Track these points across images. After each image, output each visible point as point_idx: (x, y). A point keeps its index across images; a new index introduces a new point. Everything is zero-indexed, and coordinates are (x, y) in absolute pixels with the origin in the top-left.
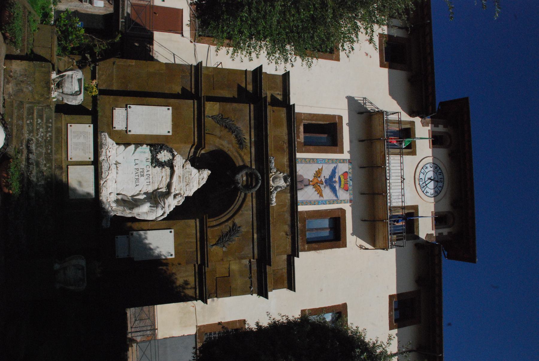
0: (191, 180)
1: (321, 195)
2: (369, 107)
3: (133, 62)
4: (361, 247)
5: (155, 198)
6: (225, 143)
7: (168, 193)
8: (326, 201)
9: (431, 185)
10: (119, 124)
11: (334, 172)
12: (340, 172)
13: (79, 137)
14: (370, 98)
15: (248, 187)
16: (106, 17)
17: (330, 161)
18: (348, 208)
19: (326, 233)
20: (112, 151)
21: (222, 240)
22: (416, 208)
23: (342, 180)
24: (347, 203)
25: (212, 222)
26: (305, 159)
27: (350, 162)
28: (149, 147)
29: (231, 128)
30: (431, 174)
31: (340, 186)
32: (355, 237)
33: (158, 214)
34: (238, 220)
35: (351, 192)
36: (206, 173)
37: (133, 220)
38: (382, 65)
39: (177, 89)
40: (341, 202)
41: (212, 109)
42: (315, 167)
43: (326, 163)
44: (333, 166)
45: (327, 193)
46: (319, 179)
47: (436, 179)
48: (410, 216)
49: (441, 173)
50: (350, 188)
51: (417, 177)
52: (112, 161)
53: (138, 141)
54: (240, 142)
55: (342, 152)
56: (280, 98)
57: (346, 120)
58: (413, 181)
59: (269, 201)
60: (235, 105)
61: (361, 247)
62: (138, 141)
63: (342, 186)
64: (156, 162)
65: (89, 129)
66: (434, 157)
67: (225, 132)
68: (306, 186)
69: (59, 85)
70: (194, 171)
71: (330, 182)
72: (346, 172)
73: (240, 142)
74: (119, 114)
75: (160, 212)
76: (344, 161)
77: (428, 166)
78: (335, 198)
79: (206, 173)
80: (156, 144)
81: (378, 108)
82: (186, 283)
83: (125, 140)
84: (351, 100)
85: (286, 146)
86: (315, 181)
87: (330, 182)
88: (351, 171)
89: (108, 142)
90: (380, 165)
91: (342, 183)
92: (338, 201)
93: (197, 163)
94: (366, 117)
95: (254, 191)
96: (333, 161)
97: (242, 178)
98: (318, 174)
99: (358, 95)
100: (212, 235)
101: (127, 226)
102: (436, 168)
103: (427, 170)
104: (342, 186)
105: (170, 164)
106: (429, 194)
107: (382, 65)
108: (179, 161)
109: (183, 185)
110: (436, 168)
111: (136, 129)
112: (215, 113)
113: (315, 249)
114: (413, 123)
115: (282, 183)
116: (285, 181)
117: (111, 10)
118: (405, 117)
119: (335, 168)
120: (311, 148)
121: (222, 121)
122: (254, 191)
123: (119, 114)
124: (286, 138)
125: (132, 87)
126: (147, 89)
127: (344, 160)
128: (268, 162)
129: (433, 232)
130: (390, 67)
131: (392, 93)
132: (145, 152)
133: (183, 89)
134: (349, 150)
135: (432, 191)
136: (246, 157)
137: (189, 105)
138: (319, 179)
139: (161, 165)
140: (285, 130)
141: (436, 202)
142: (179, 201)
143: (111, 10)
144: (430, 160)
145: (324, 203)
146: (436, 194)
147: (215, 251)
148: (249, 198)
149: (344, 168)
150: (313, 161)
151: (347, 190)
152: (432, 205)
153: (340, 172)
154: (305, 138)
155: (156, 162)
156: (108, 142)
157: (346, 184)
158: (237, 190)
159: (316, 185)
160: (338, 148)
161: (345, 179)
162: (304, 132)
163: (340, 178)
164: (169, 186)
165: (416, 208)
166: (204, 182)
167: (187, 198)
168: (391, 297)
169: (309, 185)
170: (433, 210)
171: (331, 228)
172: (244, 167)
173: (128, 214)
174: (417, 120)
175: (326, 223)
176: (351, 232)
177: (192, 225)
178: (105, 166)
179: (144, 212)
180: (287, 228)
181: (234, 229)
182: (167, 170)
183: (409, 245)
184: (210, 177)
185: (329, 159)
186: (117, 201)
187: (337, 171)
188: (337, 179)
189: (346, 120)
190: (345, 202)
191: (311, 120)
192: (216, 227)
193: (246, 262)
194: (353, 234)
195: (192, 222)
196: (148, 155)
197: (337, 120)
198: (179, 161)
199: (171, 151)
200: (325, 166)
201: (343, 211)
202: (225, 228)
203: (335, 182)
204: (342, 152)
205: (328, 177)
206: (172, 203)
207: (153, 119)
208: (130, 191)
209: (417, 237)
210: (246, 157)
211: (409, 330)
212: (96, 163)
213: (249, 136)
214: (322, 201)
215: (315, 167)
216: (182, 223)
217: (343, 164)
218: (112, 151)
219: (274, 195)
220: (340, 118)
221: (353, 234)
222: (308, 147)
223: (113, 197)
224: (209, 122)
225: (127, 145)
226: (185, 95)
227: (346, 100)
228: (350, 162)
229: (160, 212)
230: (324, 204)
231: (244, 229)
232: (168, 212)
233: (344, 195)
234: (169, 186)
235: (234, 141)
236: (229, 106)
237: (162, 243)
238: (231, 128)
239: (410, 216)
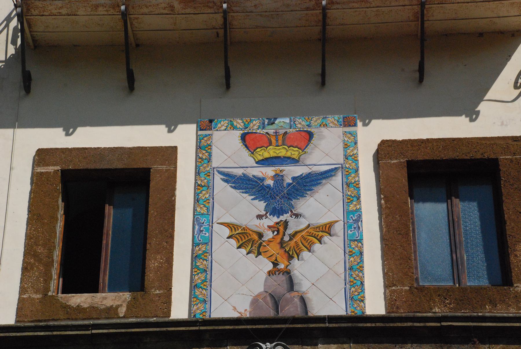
1: (327, 229)
8: (347, 213)
12: (244, 163)
17: (204, 195)
18: (372, 134)
19: (470, 213)
23: (271, 152)
24: (354, 135)
26: (193, 286)
27: (206, 125)
31: (295, 161)
32: (482, 107)
35: (316, 121)
40: (351, 157)
42: (225, 251)
43: (210, 211)
45: (319, 207)
46: (269, 235)
50: (301, 123)
55: (170, 154)
57: (54, 138)
63: (294, 153)
68: (291, 284)
71: (280, 197)
72: (243, 137)
76: (203, 148)
81: (9, 19)
86: (274, 249)
87: (280, 197)
88: (239, 123)
90: (219, 18)
91: (282, 152)
92: (349, 170)
96: (203, 188)
98: (248, 240)
104: (294, 153)
119: (229, 178)
120: (153, 263)
127: (199, 147)
134: (162, 129)
138: (269, 235)
145: (354, 219)
149: (228, 147)
151: (310, 135)
153: (244, 163)
154: (112, 289)
157: (285, 139)
159: (290, 246)
162: (93, 287)
169: (287, 273)
171: (449, 195)
175: (430, 214)
176: (463, 120)
185: (197, 200)
187: (239, 172)
188: (269, 172)
189: (54, 138)
190: (350, 145)
191: (49, 265)
194: (473, 115)
197: (51, 169)
200: (221, 214)
201: (385, 150)
203: (278, 178)
204: (170, 154)
205: (261, 205)
214: (347, 226)
215: (225, 251)
217: (215, 151)
220: (43, 156)
221: (473, 115)
222: (150, 276)
228: (206, 125)
230: (359, 219)
233: (326, 148)
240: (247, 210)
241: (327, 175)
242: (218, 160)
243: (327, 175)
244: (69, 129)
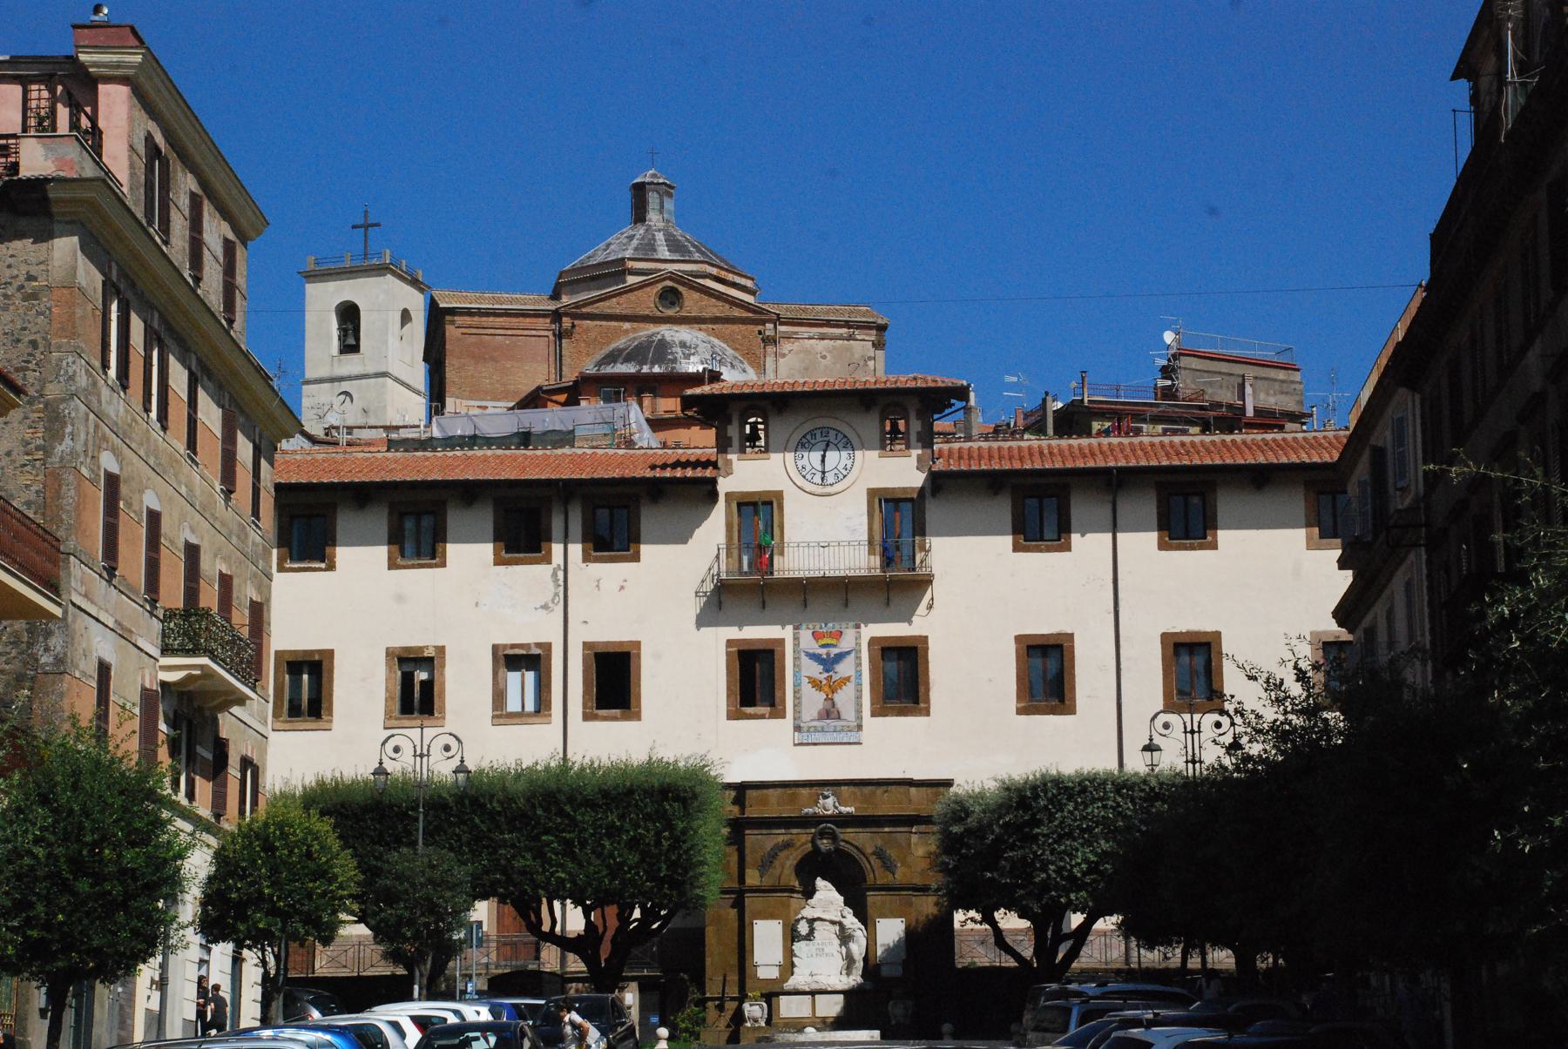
0: (827, 899)
1: (848, 679)
4: (930, 607)
5: (845, 937)
6: (788, 863)
7: (840, 924)
9: (832, 456)
11: (815, 657)
14: (695, 586)
15: (834, 837)
16: (642, 990)
21: (889, 867)
23: (825, 641)
25: (870, 878)
28: (797, 947)
29: (773, 855)
32: (914, 619)
34: (869, 850)
36: (820, 882)
38: (636, 558)
40: (858, 644)
41: (753, 878)
44: (805, 660)
45: (844, 669)
47: (823, 445)
48: (887, 503)
49: (812, 433)
51: (820, 490)
54: (787, 845)
55: (781, 642)
56: (733, 794)
57: (734, 633)
58: (826, 509)
59: (849, 815)
60: (747, 851)
61: (930, 607)
64: (809, 937)
66: (785, 449)
67: (777, 863)
68: (834, 705)
70: (817, 896)
71: (829, 663)
73: (787, 845)
76: (796, 638)
77: (800, 463)
79: (820, 882)
80: (792, 936)
84: (703, 621)
85: (789, 791)
87: (829, 663)
91: (829, 641)
93: (809, 892)
94: (723, 599)
95: (838, 830)
97: (825, 844)
98: (816, 684)
99: (693, 607)
100: (882, 878)
102: (803, 446)
103: (808, 468)
105: (811, 921)
106: (849, 463)
107: (636, 558)
108: (808, 912)
109: (832, 908)
110: (803, 445)
112: (757, 873)
113: (928, 690)
118: (720, 507)
119: (808, 654)
120: (778, 694)
122: (838, 830)
128: (807, 817)
130: (638, 541)
131: (683, 538)
133: (733, 907)
135: (844, 454)
136: (802, 839)
137: (751, 902)
140: (771, 791)
141: (864, 446)
142: (848, 912)
143: (634, 985)
144: (790, 456)
145: (859, 675)
146: (848, 445)
147: (901, 875)
148: (846, 837)
149: (806, 635)
150: (796, 692)
155: (809, 937)
157: (831, 635)
158: (838, 851)
160: (778, 649)
161: (823, 636)
163: (823, 646)
164: (833, 923)
166: (830, 886)
167: (846, 903)
168: (1017, 548)
172: (813, 841)
181: (880, 854)
182: (817, 924)
183: (934, 512)
188: (823, 651)
189: (734, 633)
190: (858, 638)
192: (876, 873)
193: (914, 838)
194: (910, 622)
195: (870, 900)
196: (803, 943)
198: (808, 912)
200: (805, 672)
201: (873, 641)
204: (781, 642)
206: (851, 921)
210: (802, 839)
211: (1078, 512)
213: (780, 836)
215: (807, 688)
216: (870, 911)
220: (730, 643)
221: (910, 622)
222: (777, 700)
224: (767, 882)
226: (739, 904)
231: (879, 843)
233: (846, 643)
234: (833, 923)
236: (748, 859)
238: (773, 855)
239: (887, 503)
240: (815, 670)
241: (848, 653)
242: (803, 645)
243: (848, 653)
244: (740, 627)
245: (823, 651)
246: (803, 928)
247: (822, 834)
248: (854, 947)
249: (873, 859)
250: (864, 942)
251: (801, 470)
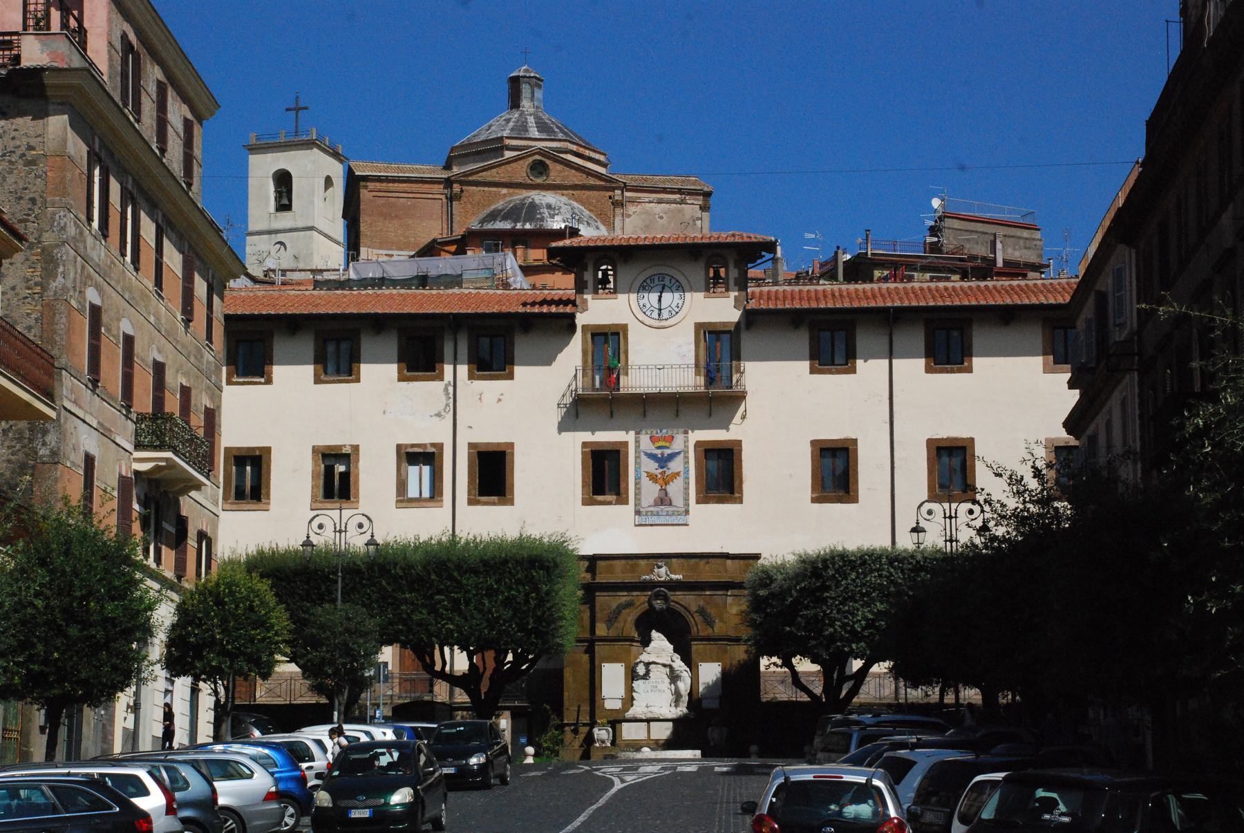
0: (660, 647)
1: (678, 474)
2: (568, 400)
3: (566, 694)
4: (744, 417)
5: (674, 677)
6: (629, 619)
7: (670, 666)
9: (667, 297)
10: (618, 705)
11: (652, 456)
13: (630, 732)
14: (557, 399)
15: (666, 599)
16: (513, 717)
20: (637, 710)
21: (709, 622)
22: (699, 327)
30: (654, 297)
33: (686, 675)
34: (694, 608)
36: (654, 634)
37: (690, 694)
38: (510, 376)
39: (586, 657)
40: (686, 447)
41: (601, 630)
45: (675, 466)
47: (660, 288)
48: (710, 334)
49: (651, 278)
51: (656, 324)
52: (646, 710)
53: (630, 690)
54: (629, 605)
55: (626, 444)
58: (662, 339)
59: (678, 582)
60: (597, 609)
61: (744, 417)
62: (630, 690)
64: (646, 676)
65: (625, 725)
66: (629, 291)
67: (621, 618)
69: (603, 742)
70: (652, 644)
71: (663, 461)
74: (609, 705)
75: (685, 674)
76: (637, 441)
77: (641, 302)
78: (682, 455)
79: (654, 634)
80: (632, 676)
82: (746, 652)
83: (629, 700)
84: (563, 427)
87: (663, 461)
89: (630, 713)
93: (646, 642)
94: (580, 410)
95: (669, 593)
97: (659, 604)
98: (652, 477)
99: (555, 416)
100: (704, 631)
101: (695, 701)
103: (648, 306)
105: (647, 665)
106: (681, 302)
107: (510, 376)
108: (645, 657)
110: (644, 288)
111: (621, 691)
114: (585, 328)
115: (663, 570)
116: (660, 567)
117: (507, 713)
119: (646, 454)
121: (611, 620)
122: (669, 593)
123: (609, 705)
124: (623, 562)
125: (586, 694)
126: (587, 683)
129: (733, 294)
130: (512, 363)
131: (548, 361)
132: (638, 685)
133: (586, 652)
135: (677, 295)
136: (641, 600)
137: (599, 649)
139: (648, 672)
141: (692, 290)
142: (677, 657)
143: (507, 713)
144: (633, 296)
146: (680, 288)
147: (719, 628)
149: (645, 439)
152: (695, 294)
155: (646, 676)
156: (630, 713)
157: (665, 439)
159: (666, 480)
160: (622, 450)
161: (659, 440)
162: (603, 494)
164: (664, 665)
165: (699, 327)
167: (675, 651)
170: (702, 294)
172: (649, 602)
173: (685, 699)
174: (581, 319)
177: (696, 647)
178: (650, 716)
179: (684, 686)
180: (703, 562)
181: (702, 611)
182: (652, 667)
184: (658, 631)
186: (676, 706)
188: (659, 452)
190: (686, 441)
192: (698, 627)
194: (728, 429)
195: (694, 648)
196: (640, 682)
198: (645, 657)
199: (637, 664)
200: (644, 468)
201: (698, 444)
202: (698, 618)
203: (662, 454)
204: (626, 444)
205: (656, 465)
206: (679, 664)
207: (612, 677)
208: (669, 697)
209: (738, 324)
210: (641, 599)
212: (648, 721)
213: (623, 597)
215: (645, 480)
216: (694, 656)
218: (637, 710)
219: (673, 576)
220: (585, 444)
221: (728, 429)
223: (673, 709)
225: (633, 699)
226: (590, 651)
227: (563, 434)
229: (685, 674)
231: (702, 603)
232: (686, 668)
233: (677, 445)
234: (664, 665)
235: (627, 610)
236: (598, 615)
237: (710, 672)
239: (710, 334)
240: (652, 466)
241: (679, 453)
242: (642, 447)
243: (679, 453)
244: (593, 432)
245: (659, 452)
246: (641, 670)
247: (657, 596)
248: (681, 685)
249: (697, 616)
250: (689, 681)
251: (642, 308)
